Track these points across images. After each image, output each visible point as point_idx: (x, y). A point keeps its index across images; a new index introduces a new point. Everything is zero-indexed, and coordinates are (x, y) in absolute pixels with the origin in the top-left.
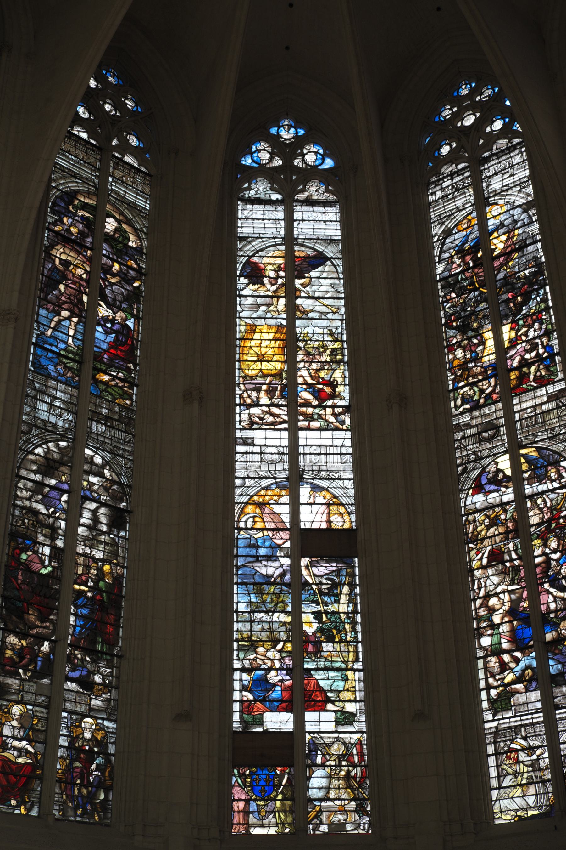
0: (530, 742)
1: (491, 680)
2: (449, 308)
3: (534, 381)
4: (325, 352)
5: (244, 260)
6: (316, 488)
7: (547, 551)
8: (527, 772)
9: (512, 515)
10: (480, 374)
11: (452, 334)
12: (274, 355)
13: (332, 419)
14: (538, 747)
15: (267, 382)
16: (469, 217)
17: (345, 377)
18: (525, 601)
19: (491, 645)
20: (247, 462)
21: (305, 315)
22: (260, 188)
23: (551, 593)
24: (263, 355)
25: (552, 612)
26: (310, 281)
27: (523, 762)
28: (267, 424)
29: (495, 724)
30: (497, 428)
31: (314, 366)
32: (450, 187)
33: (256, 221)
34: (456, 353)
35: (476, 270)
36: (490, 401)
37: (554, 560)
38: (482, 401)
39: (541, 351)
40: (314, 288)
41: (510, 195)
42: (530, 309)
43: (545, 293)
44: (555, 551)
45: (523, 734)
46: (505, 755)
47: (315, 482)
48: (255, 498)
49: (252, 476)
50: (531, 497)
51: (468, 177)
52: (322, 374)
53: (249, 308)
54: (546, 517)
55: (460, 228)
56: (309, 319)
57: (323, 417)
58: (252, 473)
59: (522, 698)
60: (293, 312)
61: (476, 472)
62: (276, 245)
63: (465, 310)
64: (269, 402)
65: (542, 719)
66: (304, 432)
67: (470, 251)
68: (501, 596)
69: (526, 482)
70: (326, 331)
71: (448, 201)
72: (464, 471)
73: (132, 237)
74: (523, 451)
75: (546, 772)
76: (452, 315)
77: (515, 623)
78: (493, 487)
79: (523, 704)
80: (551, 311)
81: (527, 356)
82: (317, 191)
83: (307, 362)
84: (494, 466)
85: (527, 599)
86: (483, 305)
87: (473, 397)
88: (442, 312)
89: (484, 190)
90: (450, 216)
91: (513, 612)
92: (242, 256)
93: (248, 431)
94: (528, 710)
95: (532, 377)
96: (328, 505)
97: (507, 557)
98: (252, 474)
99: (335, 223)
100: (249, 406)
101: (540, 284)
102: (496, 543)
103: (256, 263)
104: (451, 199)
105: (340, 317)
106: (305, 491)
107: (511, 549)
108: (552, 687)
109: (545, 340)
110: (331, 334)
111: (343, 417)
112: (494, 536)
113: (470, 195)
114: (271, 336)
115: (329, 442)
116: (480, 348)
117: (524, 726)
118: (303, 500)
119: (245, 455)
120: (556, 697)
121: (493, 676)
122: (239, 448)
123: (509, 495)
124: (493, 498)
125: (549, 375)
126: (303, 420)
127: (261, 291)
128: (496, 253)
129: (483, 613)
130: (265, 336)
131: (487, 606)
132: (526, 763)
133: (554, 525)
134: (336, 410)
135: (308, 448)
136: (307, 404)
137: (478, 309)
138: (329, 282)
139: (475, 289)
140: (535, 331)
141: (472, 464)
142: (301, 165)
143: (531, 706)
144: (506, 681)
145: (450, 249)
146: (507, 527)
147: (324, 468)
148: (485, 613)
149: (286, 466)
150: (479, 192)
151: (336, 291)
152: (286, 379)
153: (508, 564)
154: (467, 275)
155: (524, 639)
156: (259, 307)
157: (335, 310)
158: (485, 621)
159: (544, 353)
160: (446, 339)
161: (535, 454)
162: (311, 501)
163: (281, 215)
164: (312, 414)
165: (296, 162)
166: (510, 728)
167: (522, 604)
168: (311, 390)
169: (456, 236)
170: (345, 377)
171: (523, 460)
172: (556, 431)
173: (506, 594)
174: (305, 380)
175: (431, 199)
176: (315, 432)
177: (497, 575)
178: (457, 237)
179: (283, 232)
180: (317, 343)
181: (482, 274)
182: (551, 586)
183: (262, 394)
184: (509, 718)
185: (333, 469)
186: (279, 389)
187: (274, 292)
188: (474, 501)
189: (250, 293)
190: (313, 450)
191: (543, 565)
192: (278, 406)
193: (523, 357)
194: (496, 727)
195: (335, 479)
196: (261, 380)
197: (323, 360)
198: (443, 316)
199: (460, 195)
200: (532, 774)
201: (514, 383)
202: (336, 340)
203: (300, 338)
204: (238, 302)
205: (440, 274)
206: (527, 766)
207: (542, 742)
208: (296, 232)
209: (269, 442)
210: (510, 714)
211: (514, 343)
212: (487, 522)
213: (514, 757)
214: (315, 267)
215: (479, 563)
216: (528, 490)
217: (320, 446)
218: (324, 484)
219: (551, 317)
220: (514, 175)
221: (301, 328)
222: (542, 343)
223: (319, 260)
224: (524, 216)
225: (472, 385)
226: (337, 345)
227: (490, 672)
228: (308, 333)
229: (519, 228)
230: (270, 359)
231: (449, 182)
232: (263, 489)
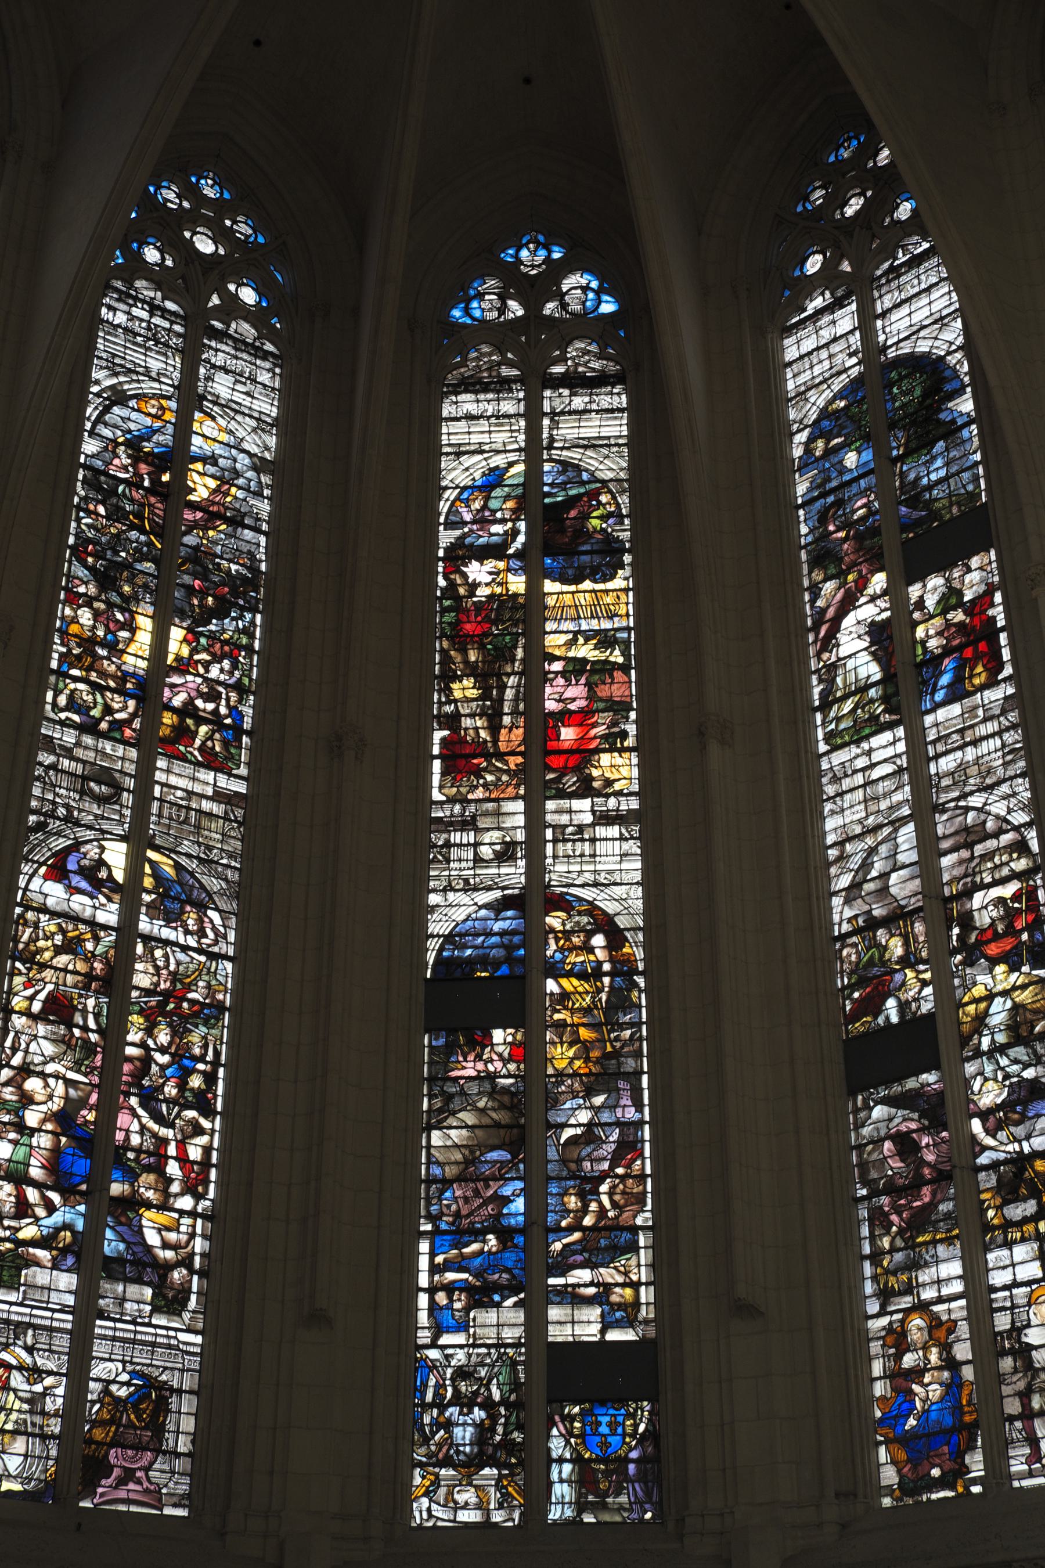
0: (38, 1359)
3: (200, 749)
7: (150, 1042)
8: (19, 1411)
9: (107, 952)
10: (114, 677)
11: (80, 574)
14: (50, 1373)
16: (163, 402)
18: (90, 1110)
19: (10, 1160)
23: (138, 1117)
25: (133, 1150)
27: (15, 1391)
30: (119, 789)
34: (79, 612)
35: (153, 500)
36: (118, 736)
37: (157, 1064)
38: (104, 726)
39: (223, 710)
41: (239, 423)
42: (224, 631)
43: (253, 622)
44: (163, 1050)
45: (29, 1341)
50: (147, 939)
51: (178, 335)
54: (162, 986)
55: (143, 405)
59: (42, 1277)
61: (60, 843)
63: (116, 553)
65: (69, 1326)
68: (51, 1081)
69: (143, 910)
71: (135, 344)
72: (40, 827)
74: (151, 854)
75: (53, 1421)
76: (89, 541)
77: (63, 1140)
78: (84, 885)
79: (42, 1288)
80: (256, 658)
81: (199, 703)
84: (97, 851)
85: (97, 1107)
86: (148, 566)
87: (90, 709)
88: (73, 524)
89: (199, 380)
91: (64, 1119)
94: (48, 1302)
95: (198, 743)
97: (78, 1019)
101: (248, 602)
102: (65, 985)
104: (140, 346)
107: (90, 1009)
109: (234, 696)
112: (65, 970)
116: (124, 634)
120: (103, 1297)
123: (109, 915)
124: (80, 904)
125: (226, 758)
128: (191, 497)
129: (8, 1097)
131: (20, 1087)
132: (20, 1394)
133: (172, 1006)
137: (138, 566)
139: (142, 531)
140: (222, 670)
141: (58, 823)
143: (54, 1297)
145: (117, 427)
146: (92, 968)
148: (14, 1098)
150: (189, 373)
153: (77, 1032)
154: (138, 495)
155: (71, 1174)
158: (9, 1112)
159: (227, 717)
161: (169, 871)
167: (84, 1112)
169: (134, 415)
171: (148, 870)
172: (214, 855)
173: (60, 1082)
177: (53, 1041)
178: (135, 420)
181: (161, 513)
182: (142, 1105)
184: (11, 1304)
188: (45, 890)
191: (137, 1063)
193: (190, 702)
198: (72, 530)
199: (158, 352)
200: (28, 1417)
201: (165, 731)
205: (87, 456)
206: (21, 1399)
207: (60, 1366)
210: (13, 1297)
211: (183, 666)
212: (58, 939)
215: (25, 1004)
216: (144, 925)
219: (252, 666)
220: (253, 397)
222: (228, 699)
224: (250, 474)
225: (95, 687)
229: (239, 488)
231: (145, 315)
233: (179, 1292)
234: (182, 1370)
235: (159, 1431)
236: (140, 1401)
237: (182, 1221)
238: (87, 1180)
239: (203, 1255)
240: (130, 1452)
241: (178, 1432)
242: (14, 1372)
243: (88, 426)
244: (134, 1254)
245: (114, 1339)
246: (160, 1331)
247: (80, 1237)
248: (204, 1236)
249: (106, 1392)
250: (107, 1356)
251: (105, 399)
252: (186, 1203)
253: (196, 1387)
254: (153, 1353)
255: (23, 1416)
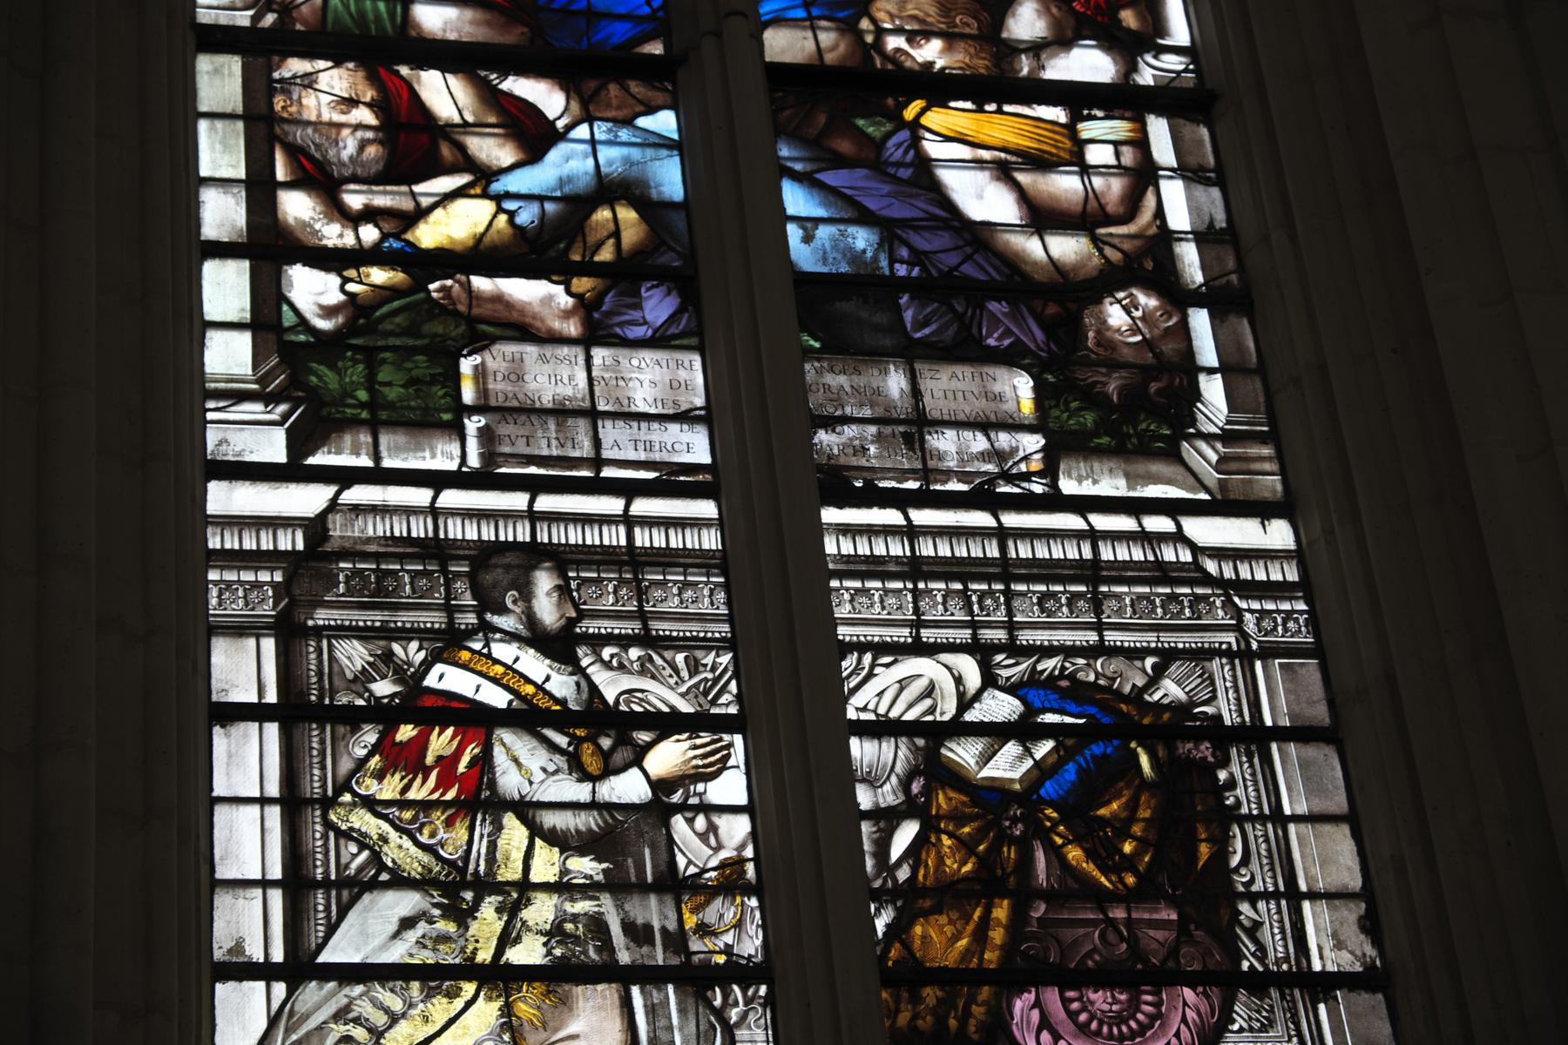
0: (599, 676)
1: (297, 206)
14: (667, 724)
27: (525, 809)
29: (308, 499)
45: (547, 610)
46: (370, 736)
59: (554, 377)
65: (711, 540)
75: (721, 911)
79: (561, 412)
108: (808, 353)
117: (562, 559)
120: (832, 423)
121: (321, 180)
132: (550, 819)
143: (618, 441)
144: (428, 235)
166: (436, 550)
184: (437, 481)
194: (316, 527)
200: (606, 906)
206: (563, 842)
210: (442, 457)
213: (447, 764)
227: (296, 153)
233: (1147, 373)
234: (1244, 656)
235: (1211, 900)
236: (1094, 787)
237: (1088, 129)
238: (657, 26)
239: (1204, 237)
240: (1100, 999)
241: (1293, 896)
242: (506, 735)
244: (918, 257)
245: (916, 569)
246: (1101, 522)
247: (679, 221)
248: (1188, 171)
249: (933, 770)
250: (903, 634)
252: (1088, 64)
253: (1320, 714)
254: (1097, 603)
255: (582, 906)
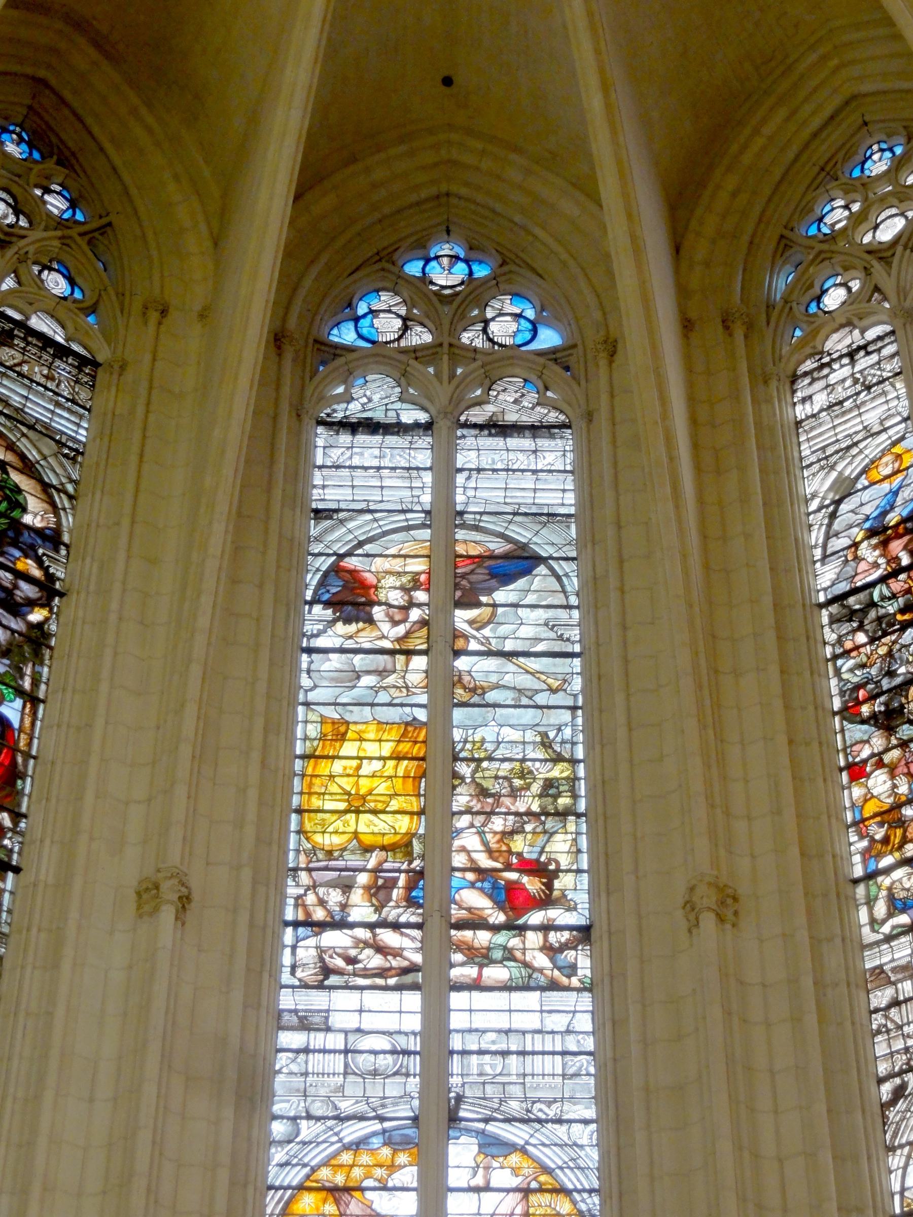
2: (851, 670)
4: (528, 787)
5: (325, 563)
6: (493, 1147)
11: (858, 736)
12: (391, 796)
13: (541, 961)
15: (371, 864)
17: (579, 851)
20: (306, 1074)
21: (478, 695)
22: (374, 395)
24: (363, 798)
26: (494, 614)
28: (366, 973)
31: (498, 824)
32: (848, 383)
33: (359, 473)
40: (503, 630)
47: (491, 1128)
48: (324, 1173)
49: (319, 1113)
52: (519, 844)
53: (332, 679)
56: (487, 705)
57: (518, 954)
58: (318, 1104)
60: (448, 690)
62: (409, 528)
64: (374, 918)
66: (465, 994)
67: (901, 530)
70: (530, 736)
71: (844, 413)
73: (33, 503)
76: (858, 687)
82: (516, 402)
83: (478, 813)
88: (834, 682)
90: (848, 448)
92: (320, 554)
93: (314, 992)
96: (526, 1192)
98: (318, 1109)
99: (562, 476)
100: (321, 926)
103: (353, 572)
104: (850, 410)
105: (570, 703)
106: (462, 1153)
110: (546, 744)
111: (570, 955)
113: (898, 398)
114: (387, 749)
115: (532, 1021)
118: (456, 1178)
119: (302, 1056)
122: (288, 1039)
126: (462, 964)
127: (366, 640)
130: (372, 749)
134: (554, 938)
135: (474, 1037)
136: (476, 923)
138: (541, 615)
142: (479, 343)
147: (516, 1091)
149: (414, 1084)
151: (561, 638)
152: (423, 857)
156: (358, 678)
157: (555, 684)
160: (845, 749)
162: (479, 1181)
163: (424, 458)
164: (489, 949)
165: (465, 338)
168: (487, 885)
169: (866, 496)
170: (579, 851)
174: (472, 860)
175: (800, 412)
176: (496, 994)
179: (426, 499)
180: (507, 766)
183: (357, 896)
185: (539, 1094)
186: (401, 882)
187: (399, 640)
189: (337, 643)
190: (488, 1041)
192: (396, 926)
195: (547, 1121)
196: (354, 860)
197: (522, 809)
198: (835, 691)
202: (558, 759)
203: (463, 755)
204: (304, 666)
205: (825, 589)
208: (460, 498)
209: (368, 1022)
214: (506, 579)
217: (507, 1032)
218: (516, 1134)
221: (465, 728)
223: (519, 562)
226: (559, 771)
228: (483, 741)
230: (380, 806)
232: (346, 1148)
243: (818, 553)
251: (827, 506)
